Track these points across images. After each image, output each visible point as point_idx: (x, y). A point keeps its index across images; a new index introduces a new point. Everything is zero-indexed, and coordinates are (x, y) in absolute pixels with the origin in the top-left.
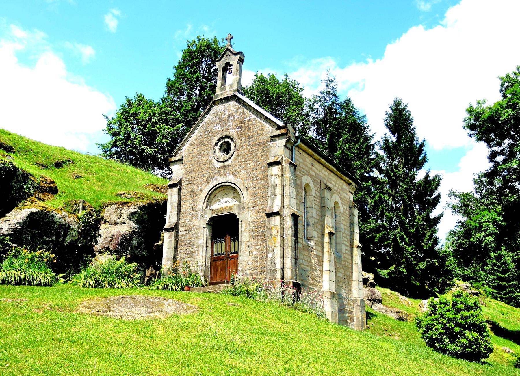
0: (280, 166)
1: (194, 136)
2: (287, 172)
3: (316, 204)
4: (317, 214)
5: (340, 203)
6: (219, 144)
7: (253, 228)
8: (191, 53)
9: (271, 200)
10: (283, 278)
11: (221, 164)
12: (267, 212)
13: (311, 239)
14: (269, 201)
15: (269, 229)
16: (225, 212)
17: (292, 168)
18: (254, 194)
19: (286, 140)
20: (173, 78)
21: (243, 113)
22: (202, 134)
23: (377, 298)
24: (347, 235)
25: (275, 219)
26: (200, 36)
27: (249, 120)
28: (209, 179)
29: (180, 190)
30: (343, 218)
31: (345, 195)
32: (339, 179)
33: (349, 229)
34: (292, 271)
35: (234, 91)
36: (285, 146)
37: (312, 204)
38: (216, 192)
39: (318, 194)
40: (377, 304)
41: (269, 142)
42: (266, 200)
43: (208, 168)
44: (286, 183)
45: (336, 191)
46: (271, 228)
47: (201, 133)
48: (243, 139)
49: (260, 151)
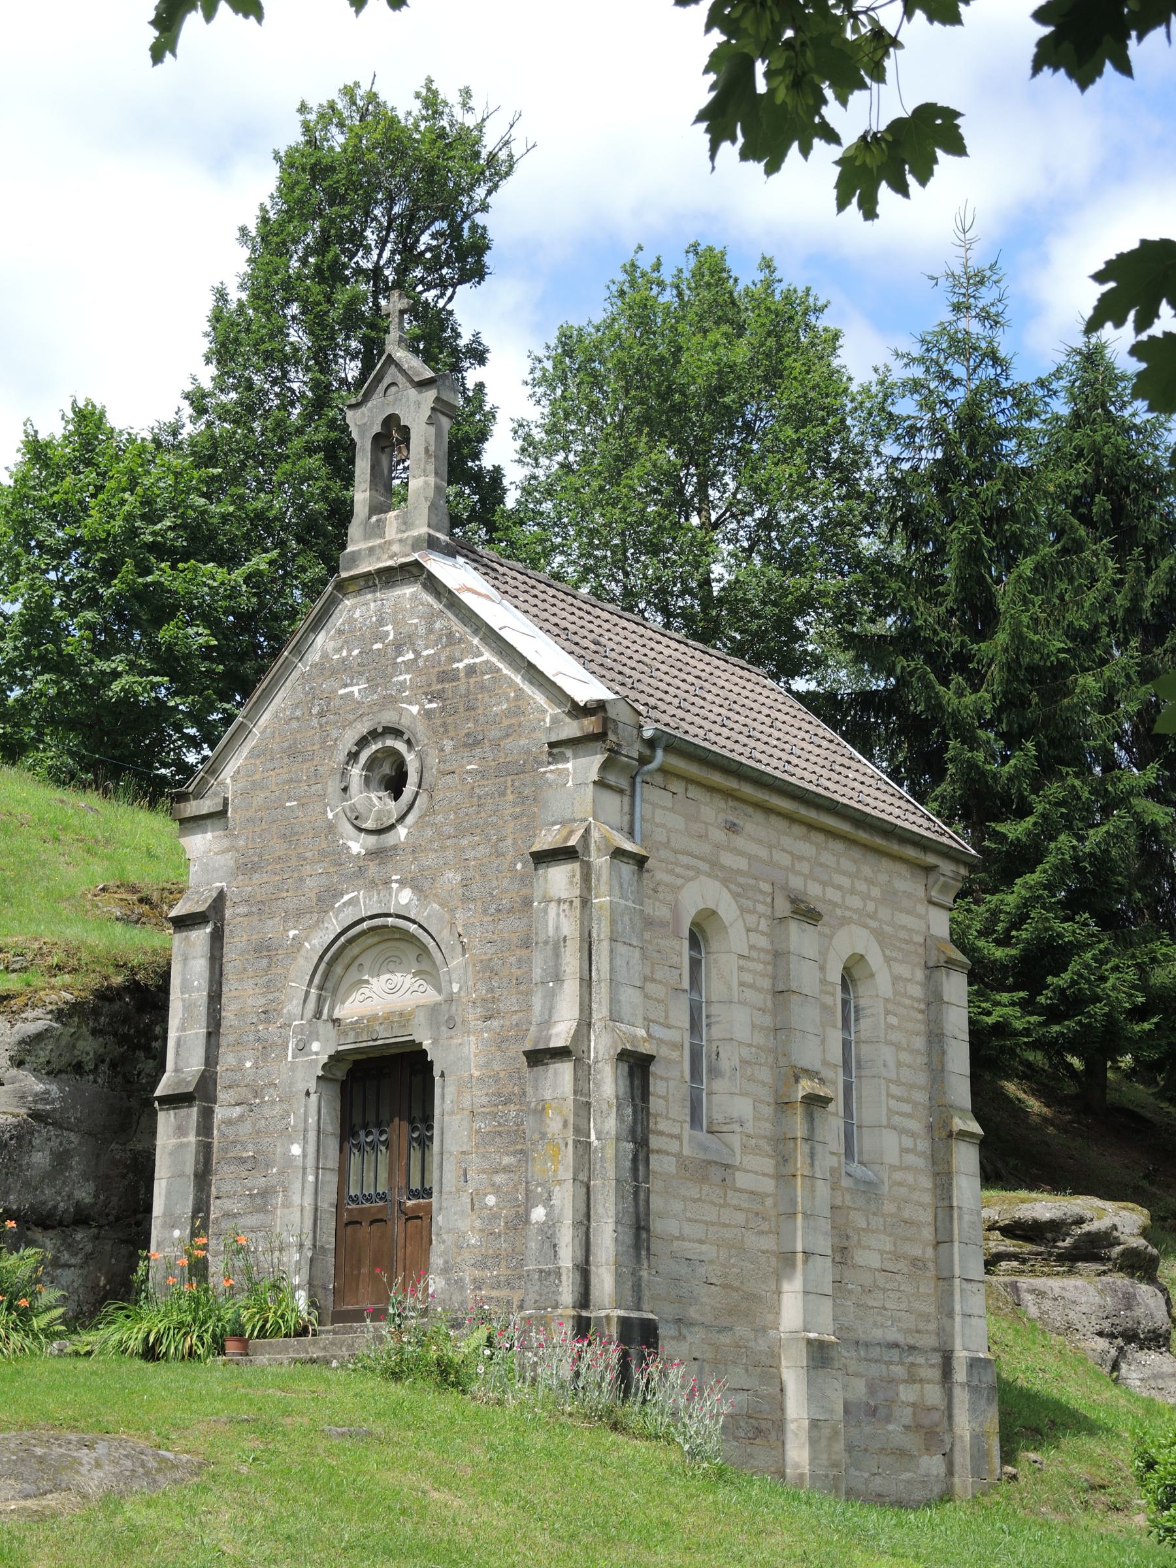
0: (576, 866)
1: (265, 718)
2: (604, 888)
3: (752, 986)
4: (753, 1026)
5: (875, 959)
6: (364, 756)
7: (484, 1100)
8: (320, 171)
9: (544, 997)
10: (584, 1300)
11: (372, 840)
12: (528, 1046)
13: (724, 1128)
14: (537, 1002)
15: (535, 1111)
16: (385, 1036)
17: (627, 869)
18: (488, 970)
19: (598, 759)
20: (236, 295)
21: (450, 635)
22: (298, 713)
23: (1146, 1325)
24: (912, 1086)
25: (556, 1073)
26: (357, 85)
27: (471, 670)
28: (327, 899)
29: (217, 937)
30: (893, 1020)
31: (904, 919)
32: (872, 859)
33: (921, 1060)
34: (618, 1276)
35: (416, 545)
36: (600, 784)
37: (729, 988)
38: (355, 949)
39: (763, 942)
40: (1142, 1356)
41: (541, 764)
42: (529, 993)
43: (323, 854)
44: (601, 931)
45: (856, 911)
46: (543, 1109)
47: (297, 706)
48: (448, 745)
49: (510, 797)
